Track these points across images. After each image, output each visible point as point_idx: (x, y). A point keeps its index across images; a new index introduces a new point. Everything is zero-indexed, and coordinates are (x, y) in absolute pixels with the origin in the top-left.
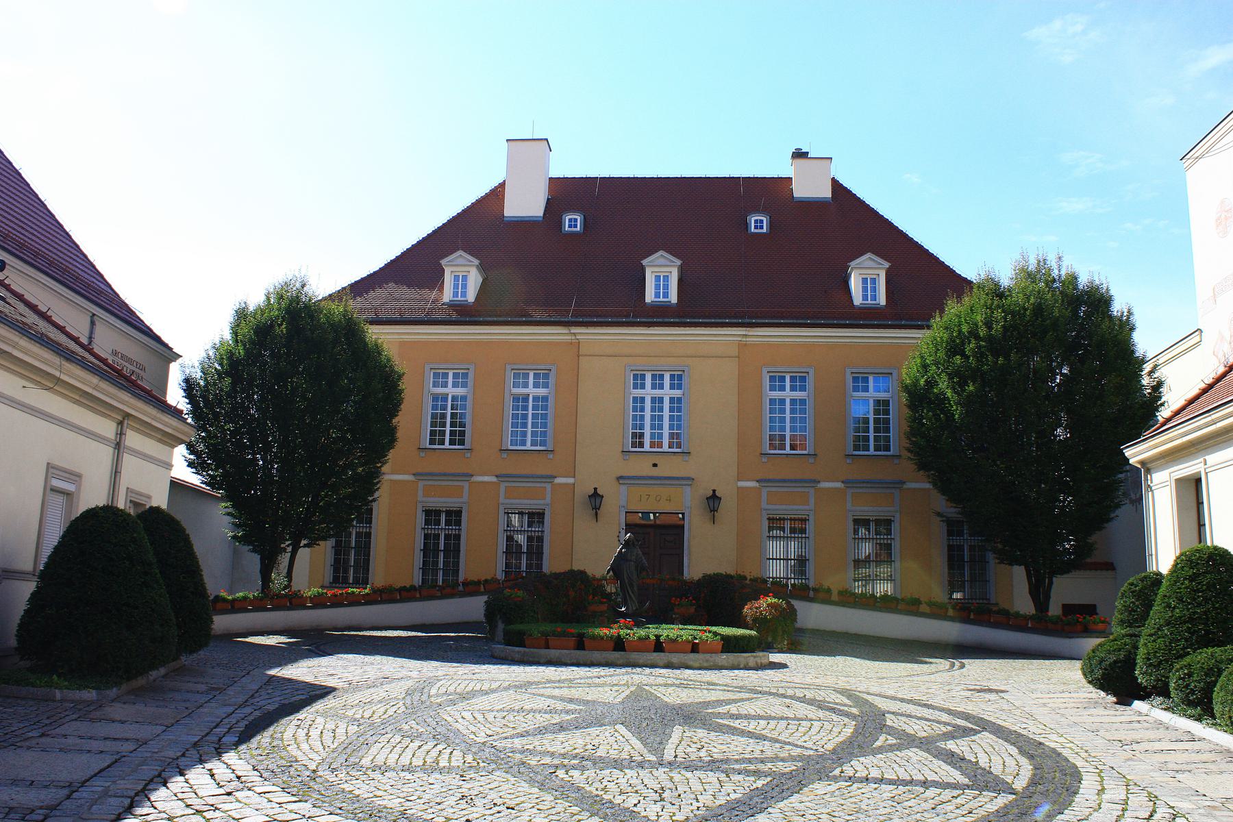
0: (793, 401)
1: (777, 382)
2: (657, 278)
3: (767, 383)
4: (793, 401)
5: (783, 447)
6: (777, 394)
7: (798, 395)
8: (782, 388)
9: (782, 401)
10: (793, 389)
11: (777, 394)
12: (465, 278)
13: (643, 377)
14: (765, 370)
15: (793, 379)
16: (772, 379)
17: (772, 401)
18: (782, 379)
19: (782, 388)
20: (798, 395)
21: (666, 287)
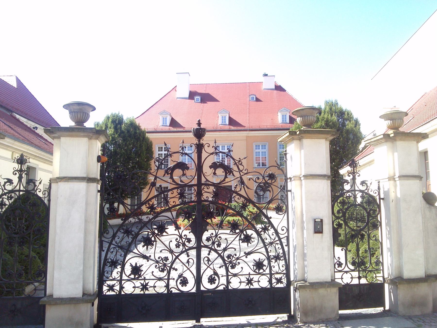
0: (262, 152)
1: (258, 147)
2: (222, 117)
3: (255, 147)
4: (262, 152)
5: (260, 166)
6: (258, 151)
7: (264, 150)
8: (259, 149)
9: (259, 152)
10: (262, 149)
11: (258, 151)
12: (166, 118)
13: (224, 146)
14: (254, 143)
15: (262, 146)
16: (256, 146)
17: (256, 153)
18: (259, 146)
19: (259, 149)
20: (264, 150)
21: (225, 120)
